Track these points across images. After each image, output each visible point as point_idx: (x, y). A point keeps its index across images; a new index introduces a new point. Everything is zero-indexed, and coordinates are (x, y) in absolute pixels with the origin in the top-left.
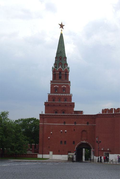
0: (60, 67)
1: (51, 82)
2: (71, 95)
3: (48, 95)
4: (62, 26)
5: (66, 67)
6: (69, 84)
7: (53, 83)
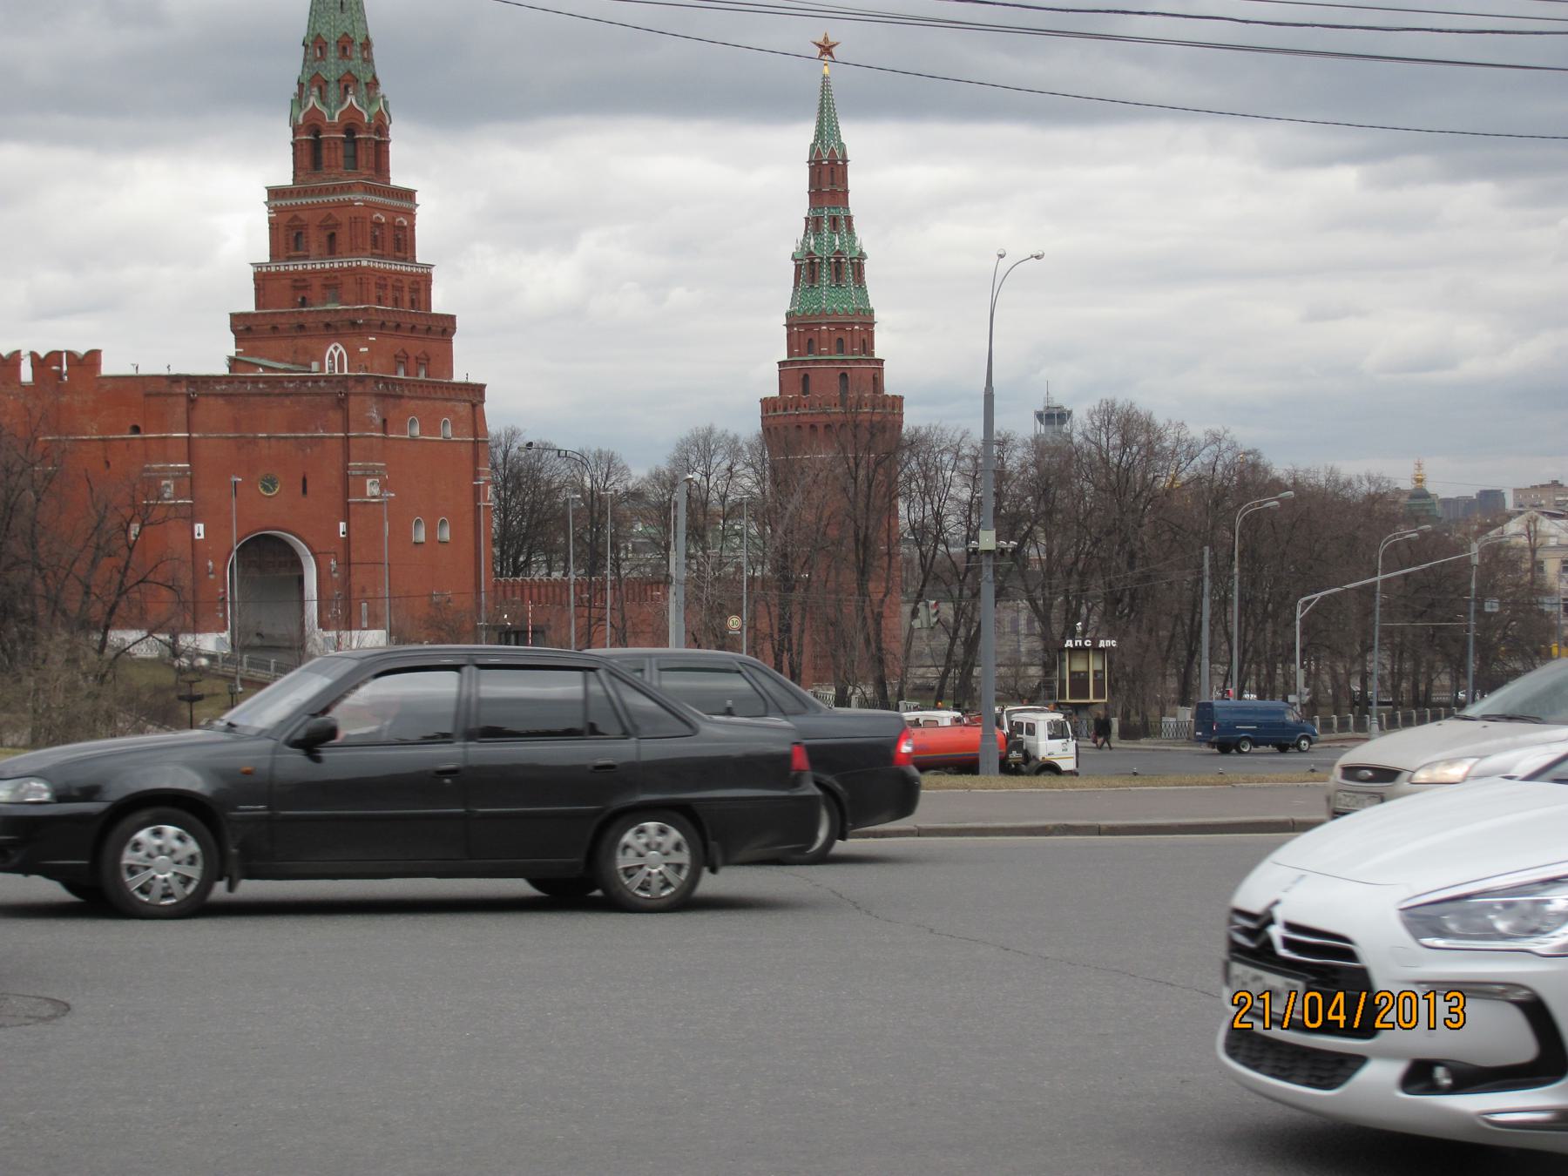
3: (251, 270)
5: (351, 99)
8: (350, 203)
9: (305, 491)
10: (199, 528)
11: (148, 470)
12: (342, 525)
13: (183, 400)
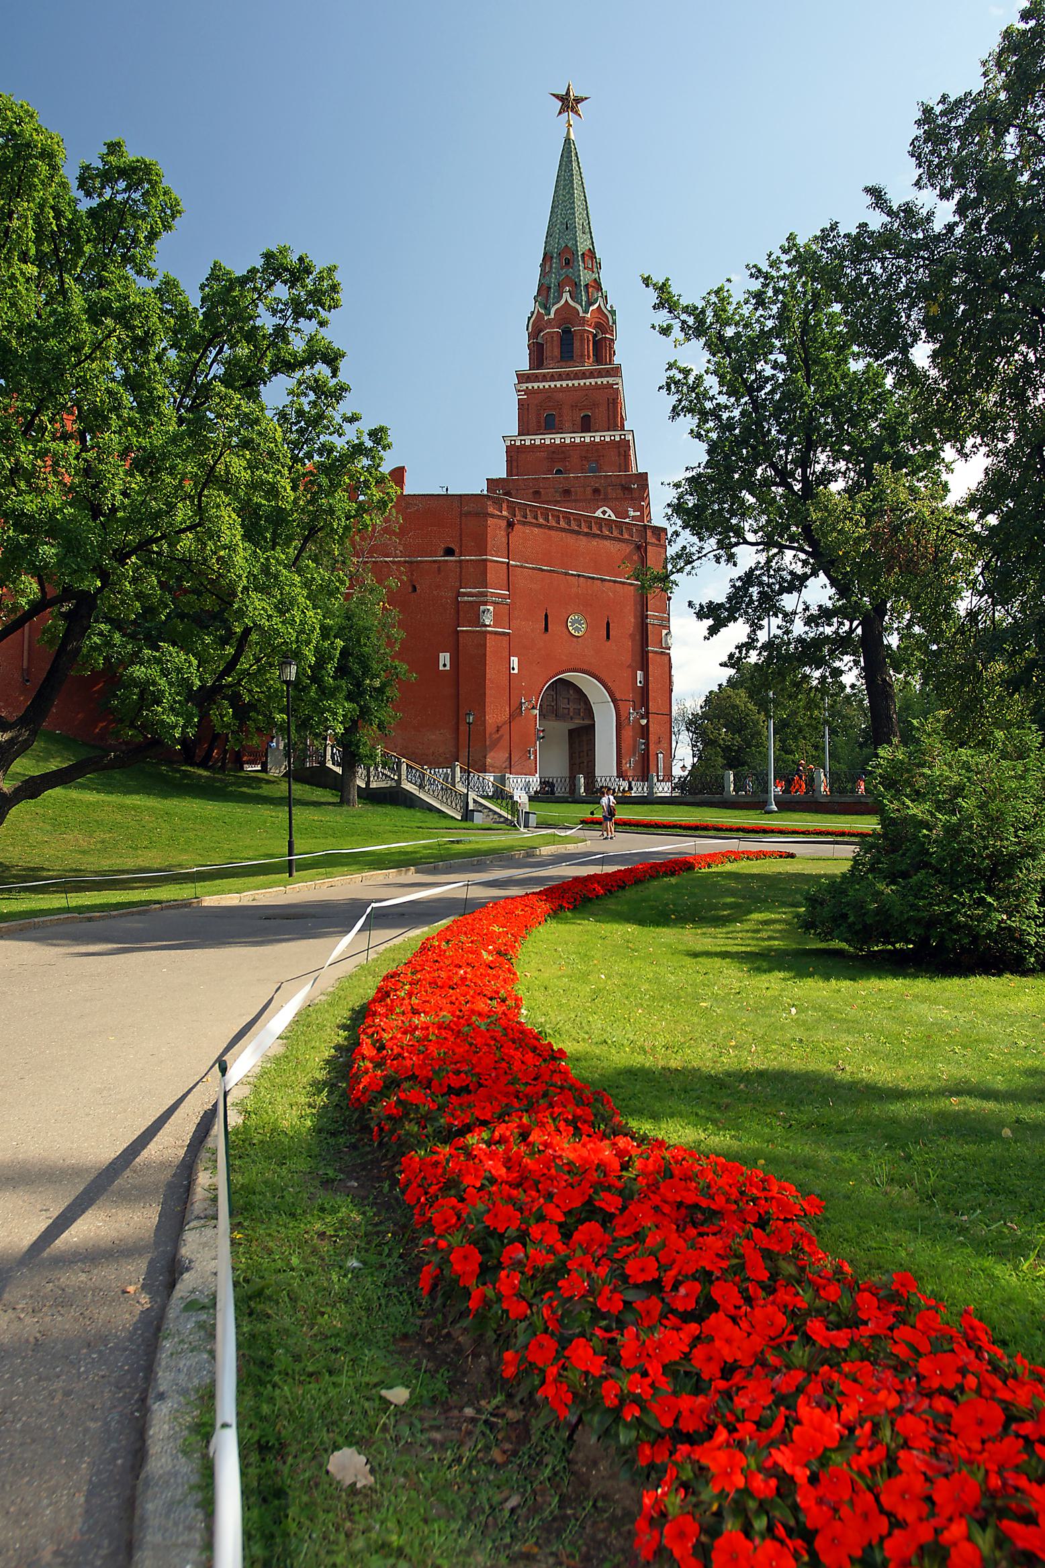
0: (566, 296)
1: (522, 378)
4: (568, 103)
6: (611, 380)
7: (530, 385)
8: (610, 386)
9: (608, 637)
10: (515, 661)
11: (465, 594)
13: (504, 524)
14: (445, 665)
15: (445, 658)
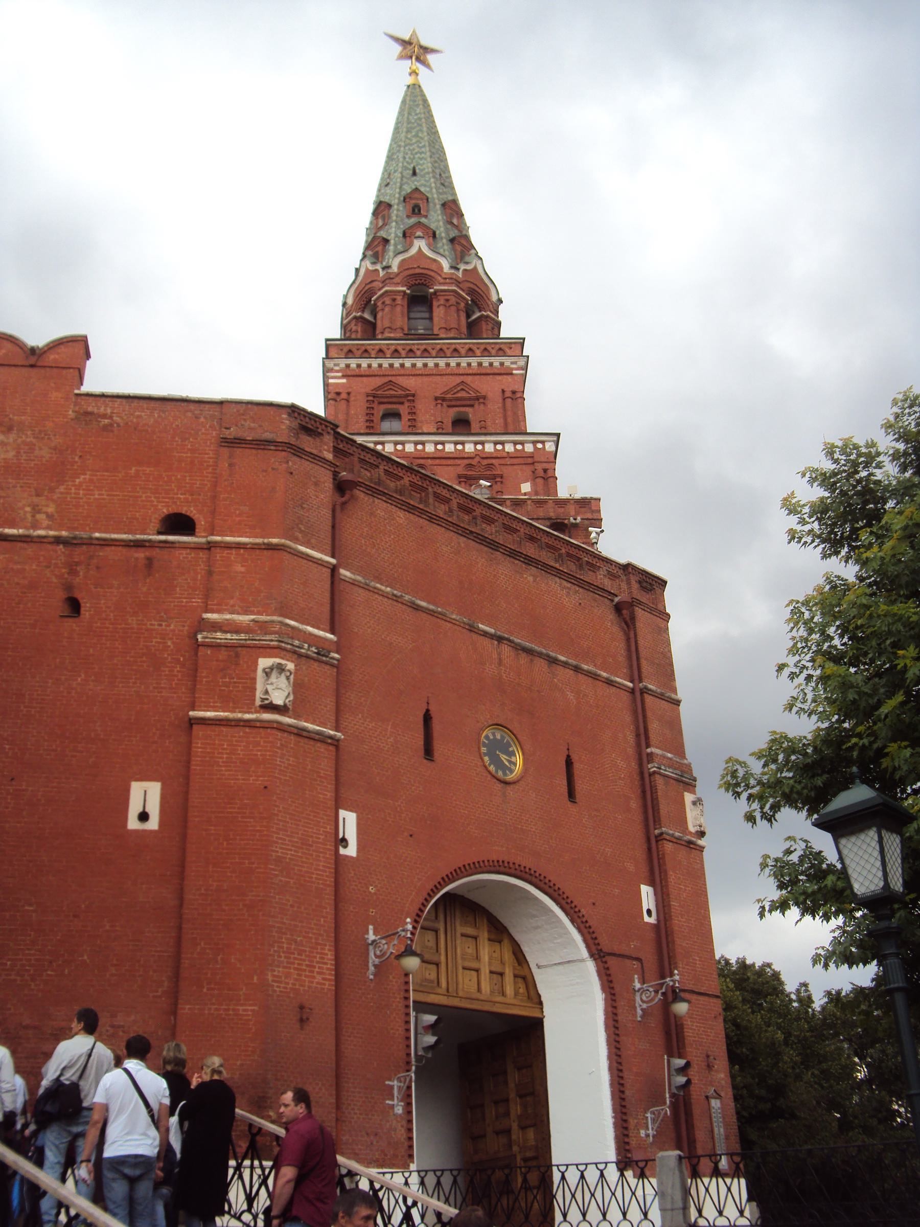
2: (549, 447)
4: (415, 51)
7: (353, 363)
9: (571, 794)
10: (349, 822)
11: (216, 627)
12: (647, 893)
14: (144, 817)
15: (146, 797)
